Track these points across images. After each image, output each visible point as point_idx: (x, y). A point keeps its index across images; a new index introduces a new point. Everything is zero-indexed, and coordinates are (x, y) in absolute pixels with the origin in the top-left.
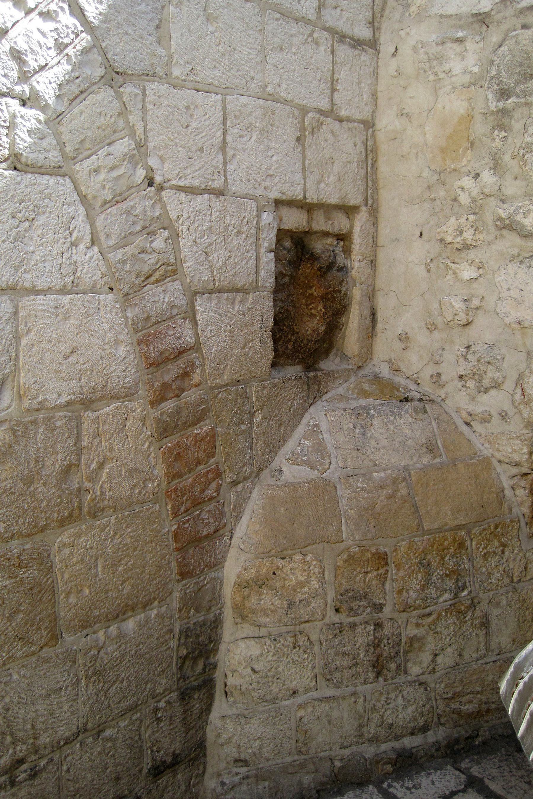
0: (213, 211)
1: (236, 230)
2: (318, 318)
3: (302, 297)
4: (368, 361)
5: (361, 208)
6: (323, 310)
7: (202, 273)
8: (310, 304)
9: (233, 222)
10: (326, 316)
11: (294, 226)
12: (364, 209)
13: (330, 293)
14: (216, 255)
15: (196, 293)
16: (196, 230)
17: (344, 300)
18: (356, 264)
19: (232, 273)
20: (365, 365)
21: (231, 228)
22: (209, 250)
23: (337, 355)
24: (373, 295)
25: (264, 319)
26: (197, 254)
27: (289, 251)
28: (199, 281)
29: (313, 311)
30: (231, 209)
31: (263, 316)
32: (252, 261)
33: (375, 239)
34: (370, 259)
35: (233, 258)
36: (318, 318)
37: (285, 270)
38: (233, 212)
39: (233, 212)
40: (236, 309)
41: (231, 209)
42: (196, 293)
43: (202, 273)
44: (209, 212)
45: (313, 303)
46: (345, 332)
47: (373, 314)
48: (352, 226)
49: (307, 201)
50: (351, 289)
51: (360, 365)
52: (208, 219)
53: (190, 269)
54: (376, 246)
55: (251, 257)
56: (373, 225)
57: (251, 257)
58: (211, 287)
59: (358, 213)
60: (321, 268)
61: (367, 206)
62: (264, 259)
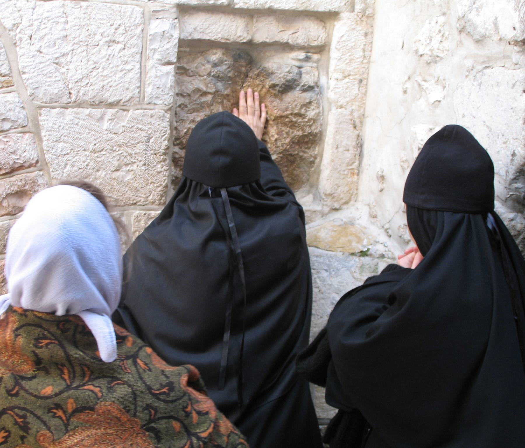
0: (69, 19)
1: (107, 39)
4: (352, 202)
5: (342, 15)
6: (276, 136)
7: (49, 86)
9: (101, 31)
10: (279, 144)
11: (220, 36)
12: (345, 15)
13: (287, 117)
14: (72, 66)
15: (40, 107)
16: (41, 39)
17: (310, 126)
18: (332, 83)
19: (97, 87)
20: (344, 207)
21: (98, 37)
22: (62, 60)
23: (309, 193)
24: (361, 123)
25: (151, 141)
26: (41, 66)
27: (215, 65)
28: (44, 94)
30: (98, 16)
31: (149, 138)
32: (134, 75)
33: (367, 54)
34: (358, 77)
35: (100, 70)
37: (207, 87)
38: (102, 19)
39: (102, 19)
40: (105, 127)
41: (98, 16)
42: (40, 107)
43: (49, 86)
44: (63, 20)
47: (360, 146)
48: (329, 37)
49: (237, 6)
51: (336, 205)
52: (60, 26)
53: (30, 81)
54: (369, 63)
55: (130, 71)
56: (366, 35)
57: (130, 71)
58: (65, 99)
59: (339, 19)
60: (274, 86)
61: (353, 10)
62: (152, 73)
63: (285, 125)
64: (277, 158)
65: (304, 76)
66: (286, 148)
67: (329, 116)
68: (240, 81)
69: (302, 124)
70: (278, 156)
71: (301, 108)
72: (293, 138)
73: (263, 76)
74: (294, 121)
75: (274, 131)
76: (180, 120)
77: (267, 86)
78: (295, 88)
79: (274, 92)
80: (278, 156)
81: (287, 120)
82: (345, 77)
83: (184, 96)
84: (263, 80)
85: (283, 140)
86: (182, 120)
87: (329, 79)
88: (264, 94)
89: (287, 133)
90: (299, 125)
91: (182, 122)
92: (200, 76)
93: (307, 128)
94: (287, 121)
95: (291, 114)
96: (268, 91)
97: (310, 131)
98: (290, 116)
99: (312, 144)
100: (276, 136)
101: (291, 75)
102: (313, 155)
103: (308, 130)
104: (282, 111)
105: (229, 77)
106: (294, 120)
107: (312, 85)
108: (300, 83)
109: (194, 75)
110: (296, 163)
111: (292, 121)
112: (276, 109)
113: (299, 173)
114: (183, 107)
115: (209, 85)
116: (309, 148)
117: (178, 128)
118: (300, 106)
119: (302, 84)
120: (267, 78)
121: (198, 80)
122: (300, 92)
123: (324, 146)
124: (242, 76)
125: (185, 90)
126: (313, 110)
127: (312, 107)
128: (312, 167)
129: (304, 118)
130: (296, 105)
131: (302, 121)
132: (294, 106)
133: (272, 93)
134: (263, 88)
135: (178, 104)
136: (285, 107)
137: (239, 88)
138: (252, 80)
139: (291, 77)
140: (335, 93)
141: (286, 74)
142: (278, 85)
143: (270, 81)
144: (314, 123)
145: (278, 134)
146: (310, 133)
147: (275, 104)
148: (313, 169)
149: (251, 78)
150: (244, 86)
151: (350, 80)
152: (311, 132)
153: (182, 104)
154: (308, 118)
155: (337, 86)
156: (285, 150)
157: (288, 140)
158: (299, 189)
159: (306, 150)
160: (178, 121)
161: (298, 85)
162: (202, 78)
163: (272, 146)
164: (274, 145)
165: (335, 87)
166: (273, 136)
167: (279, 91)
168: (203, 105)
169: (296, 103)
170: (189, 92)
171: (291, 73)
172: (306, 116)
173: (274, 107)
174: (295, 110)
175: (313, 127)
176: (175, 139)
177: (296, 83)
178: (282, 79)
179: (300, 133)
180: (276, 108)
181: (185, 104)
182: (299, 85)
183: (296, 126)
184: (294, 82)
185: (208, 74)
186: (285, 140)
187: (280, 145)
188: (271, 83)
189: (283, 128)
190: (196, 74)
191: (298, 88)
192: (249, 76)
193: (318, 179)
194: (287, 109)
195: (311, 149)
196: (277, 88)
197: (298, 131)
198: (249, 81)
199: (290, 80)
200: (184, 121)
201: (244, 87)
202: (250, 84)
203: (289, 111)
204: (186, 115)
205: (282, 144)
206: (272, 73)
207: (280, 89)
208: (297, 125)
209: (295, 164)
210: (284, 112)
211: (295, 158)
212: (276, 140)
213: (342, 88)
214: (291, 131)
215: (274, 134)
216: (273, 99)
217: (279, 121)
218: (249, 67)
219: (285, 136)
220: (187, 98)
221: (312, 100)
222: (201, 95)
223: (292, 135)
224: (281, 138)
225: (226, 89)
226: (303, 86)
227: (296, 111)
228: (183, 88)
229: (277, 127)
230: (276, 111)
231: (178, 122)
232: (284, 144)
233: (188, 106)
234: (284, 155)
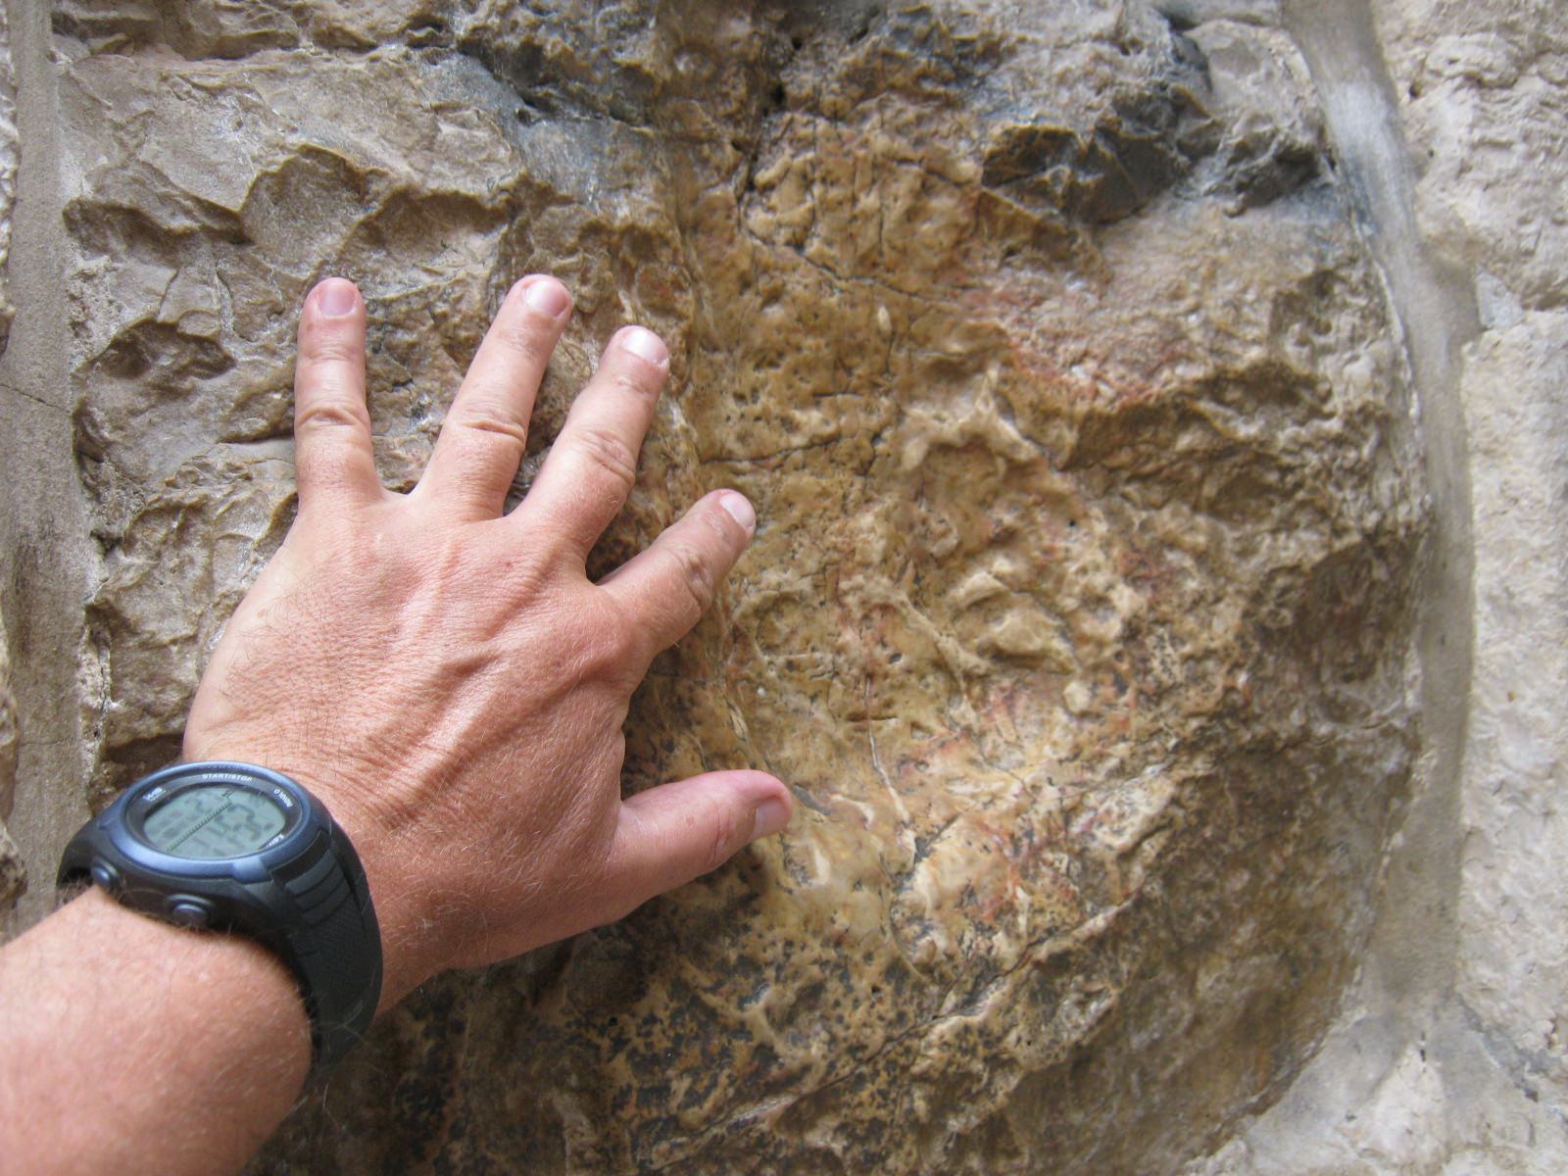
2: (1078, 693)
3: (840, 480)
6: (1126, 599)
8: (968, 555)
10: (1166, 661)
17: (1363, 475)
23: (1393, 1037)
29: (1010, 627)
36: (1078, 693)
45: (1005, 540)
46: (1446, 805)
50: (1435, 363)
63: (1175, 485)
64: (1175, 801)
65: (1221, 75)
66: (1229, 689)
67: (1472, 382)
68: (727, 133)
69: (1313, 459)
70: (1180, 773)
71: (1278, 328)
72: (1257, 598)
73: (911, 93)
74: (1245, 444)
75: (1100, 557)
76: (143, 517)
77: (969, 167)
78: (1182, 175)
79: (1037, 214)
80: (1180, 773)
81: (1184, 441)
82: (1522, 64)
83: (168, 245)
84: (920, 120)
85: (1190, 623)
86: (171, 510)
87: (1402, 89)
88: (946, 239)
89: (1201, 556)
90: (1289, 469)
91: (181, 536)
92: (333, 39)
93: (1349, 494)
94: (1190, 453)
95: (1214, 386)
96: (983, 208)
97: (1371, 520)
98: (1205, 406)
99: (1384, 626)
100: (1126, 599)
101: (1141, 60)
102: (1398, 723)
103: (1356, 511)
104: (1132, 365)
105: (632, 72)
106: (1246, 430)
107: (1304, 139)
108: (1218, 127)
109: (266, 40)
110: (1302, 811)
111: (1225, 450)
112: (1078, 360)
113: (1321, 896)
114: (182, 372)
115: (447, 130)
116: (1363, 671)
117: (135, 608)
118: (1266, 307)
119: (1235, 135)
120: (950, 104)
121: (323, 82)
122: (1231, 205)
123: (1468, 628)
124: (738, 88)
125: (183, 178)
126: (1354, 340)
127: (1343, 323)
128: (1396, 822)
129: (1316, 413)
130: (1235, 305)
131: (1304, 433)
132: (1217, 314)
133: (1011, 226)
134: (925, 190)
135: (104, 331)
136: (1148, 326)
137: (726, 191)
138: (822, 124)
139: (1141, 73)
140: (1487, 187)
141: (1105, 49)
142: (1058, 141)
143: (983, 119)
144: (1382, 444)
145: (1133, 579)
146: (1371, 537)
147: (1048, 315)
148: (1398, 839)
149: (813, 107)
150: (763, 176)
151: (1554, 89)
152: (1379, 525)
153: (156, 330)
154: (1337, 403)
155: (1492, 133)
156: (1231, 711)
157: (1225, 623)
158: (1326, 1024)
159: (1350, 691)
160: (117, 529)
161: (1200, 150)
162: (359, 64)
163: (1107, 691)
164: (1122, 689)
165: (1477, 135)
166: (1097, 601)
167: (1072, 199)
168: (403, 337)
169: (1228, 289)
170: (233, 200)
171: (1136, 44)
172: (1322, 388)
173: (1058, 337)
174: (1235, 347)
175: (1385, 485)
176: (110, 754)
177: (1185, 128)
178: (1085, 93)
179: (1304, 546)
180: (1074, 347)
181: (191, 328)
182: (1210, 150)
183: (1268, 489)
184: (1174, 123)
185: (418, 22)
186: (1206, 625)
187: (1179, 673)
188: (996, 131)
189: (1167, 520)
190: (289, 24)
191: (1208, 175)
192: (792, 90)
193: (1444, 911)
194: (1171, 346)
195: (1380, 673)
196: (1060, 173)
197: (1287, 525)
198: (803, 132)
199: (1143, 100)
200: (199, 527)
201: (769, 187)
202: (814, 164)
203: (1189, 360)
204: (222, 457)
205: (1187, 659)
206: (994, 52)
207: (1086, 180)
208: (1272, 477)
209: (1295, 828)
210: (1151, 374)
211: (1297, 772)
212: (1133, 632)
213: (1520, 148)
214: (1230, 535)
215: (1099, 580)
216: (1026, 275)
217: (1124, 456)
218: (783, 26)
219: (1191, 585)
220: (203, 259)
221: (1330, 264)
222: (373, 234)
223: (1249, 570)
224: (1165, 608)
225: (622, 181)
226: (1244, 151)
227: (1255, 354)
228: (153, 149)
229: (1111, 514)
230: (1080, 375)
231: (126, 543)
232: (1209, 653)
233: (233, 348)
234: (1220, 758)
